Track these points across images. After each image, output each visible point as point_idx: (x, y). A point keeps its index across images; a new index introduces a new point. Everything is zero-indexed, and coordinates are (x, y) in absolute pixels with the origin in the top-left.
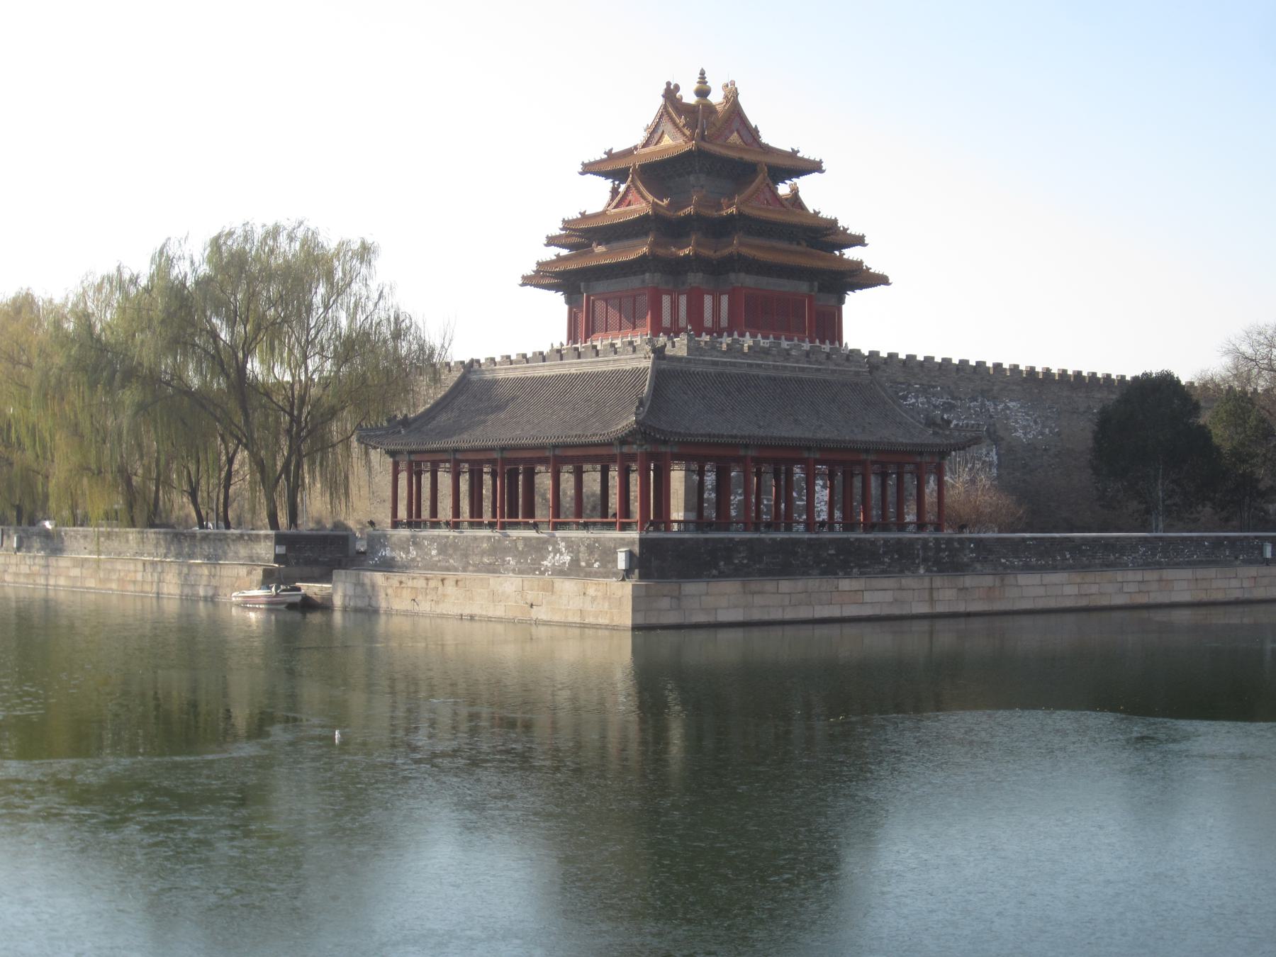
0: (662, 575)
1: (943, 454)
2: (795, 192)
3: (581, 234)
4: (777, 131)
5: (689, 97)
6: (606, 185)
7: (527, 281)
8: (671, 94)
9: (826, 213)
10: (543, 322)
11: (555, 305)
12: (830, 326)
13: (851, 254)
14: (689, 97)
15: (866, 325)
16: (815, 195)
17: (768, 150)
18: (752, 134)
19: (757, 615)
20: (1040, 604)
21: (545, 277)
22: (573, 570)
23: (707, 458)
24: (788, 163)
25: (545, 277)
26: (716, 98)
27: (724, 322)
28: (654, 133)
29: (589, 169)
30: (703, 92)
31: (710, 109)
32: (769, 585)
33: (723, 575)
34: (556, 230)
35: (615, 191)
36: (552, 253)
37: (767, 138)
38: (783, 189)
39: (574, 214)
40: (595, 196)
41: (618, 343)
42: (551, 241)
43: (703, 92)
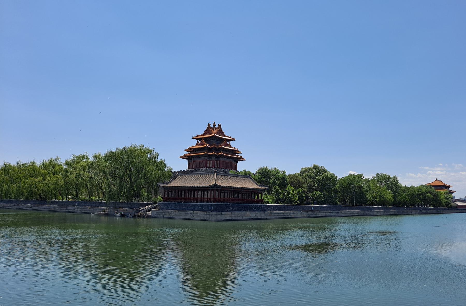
0: (219, 211)
2: (230, 143)
3: (192, 150)
4: (228, 132)
5: (212, 126)
6: (196, 141)
7: (180, 158)
9: (236, 148)
10: (184, 165)
11: (186, 161)
12: (235, 168)
13: (239, 154)
14: (212, 126)
15: (241, 167)
16: (234, 145)
18: (223, 134)
19: (234, 218)
20: (278, 217)
21: (185, 157)
22: (201, 210)
23: (225, 190)
24: (229, 138)
25: (185, 157)
26: (217, 126)
28: (206, 133)
30: (214, 126)
31: (216, 129)
32: (236, 213)
33: (228, 211)
34: (187, 148)
35: (198, 142)
37: (225, 134)
38: (228, 143)
42: (185, 151)
43: (214, 126)
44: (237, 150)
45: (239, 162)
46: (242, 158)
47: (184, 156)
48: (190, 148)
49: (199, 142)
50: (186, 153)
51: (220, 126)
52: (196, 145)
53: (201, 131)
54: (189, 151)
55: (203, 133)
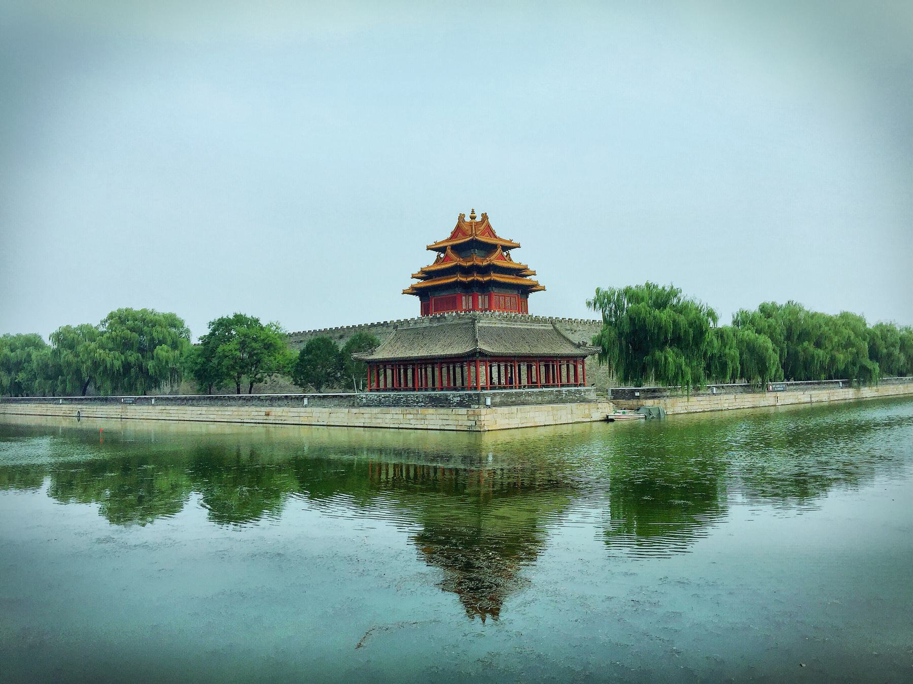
1: (585, 357)
2: (508, 254)
3: (427, 274)
4: (503, 231)
6: (435, 254)
8: (461, 217)
9: (524, 263)
10: (411, 309)
11: (416, 300)
13: (532, 277)
16: (517, 258)
17: (501, 239)
18: (492, 233)
27: (487, 307)
28: (454, 235)
29: (428, 249)
30: (473, 218)
34: (416, 270)
36: (415, 282)
37: (497, 234)
38: (505, 254)
39: (424, 266)
40: (429, 260)
41: (446, 315)
44: (526, 269)
45: (531, 295)
46: (536, 285)
47: (413, 288)
48: (423, 272)
49: (442, 255)
50: (415, 282)
51: (485, 217)
52: (437, 262)
53: (443, 233)
54: (421, 278)
55: (449, 235)
